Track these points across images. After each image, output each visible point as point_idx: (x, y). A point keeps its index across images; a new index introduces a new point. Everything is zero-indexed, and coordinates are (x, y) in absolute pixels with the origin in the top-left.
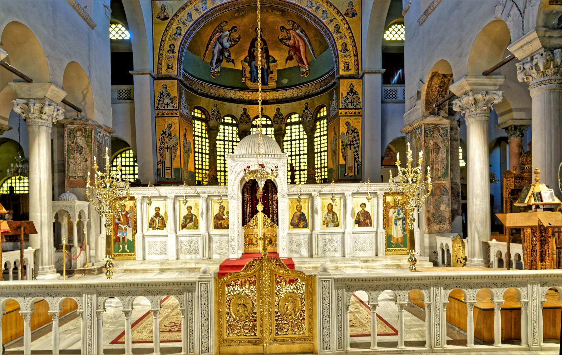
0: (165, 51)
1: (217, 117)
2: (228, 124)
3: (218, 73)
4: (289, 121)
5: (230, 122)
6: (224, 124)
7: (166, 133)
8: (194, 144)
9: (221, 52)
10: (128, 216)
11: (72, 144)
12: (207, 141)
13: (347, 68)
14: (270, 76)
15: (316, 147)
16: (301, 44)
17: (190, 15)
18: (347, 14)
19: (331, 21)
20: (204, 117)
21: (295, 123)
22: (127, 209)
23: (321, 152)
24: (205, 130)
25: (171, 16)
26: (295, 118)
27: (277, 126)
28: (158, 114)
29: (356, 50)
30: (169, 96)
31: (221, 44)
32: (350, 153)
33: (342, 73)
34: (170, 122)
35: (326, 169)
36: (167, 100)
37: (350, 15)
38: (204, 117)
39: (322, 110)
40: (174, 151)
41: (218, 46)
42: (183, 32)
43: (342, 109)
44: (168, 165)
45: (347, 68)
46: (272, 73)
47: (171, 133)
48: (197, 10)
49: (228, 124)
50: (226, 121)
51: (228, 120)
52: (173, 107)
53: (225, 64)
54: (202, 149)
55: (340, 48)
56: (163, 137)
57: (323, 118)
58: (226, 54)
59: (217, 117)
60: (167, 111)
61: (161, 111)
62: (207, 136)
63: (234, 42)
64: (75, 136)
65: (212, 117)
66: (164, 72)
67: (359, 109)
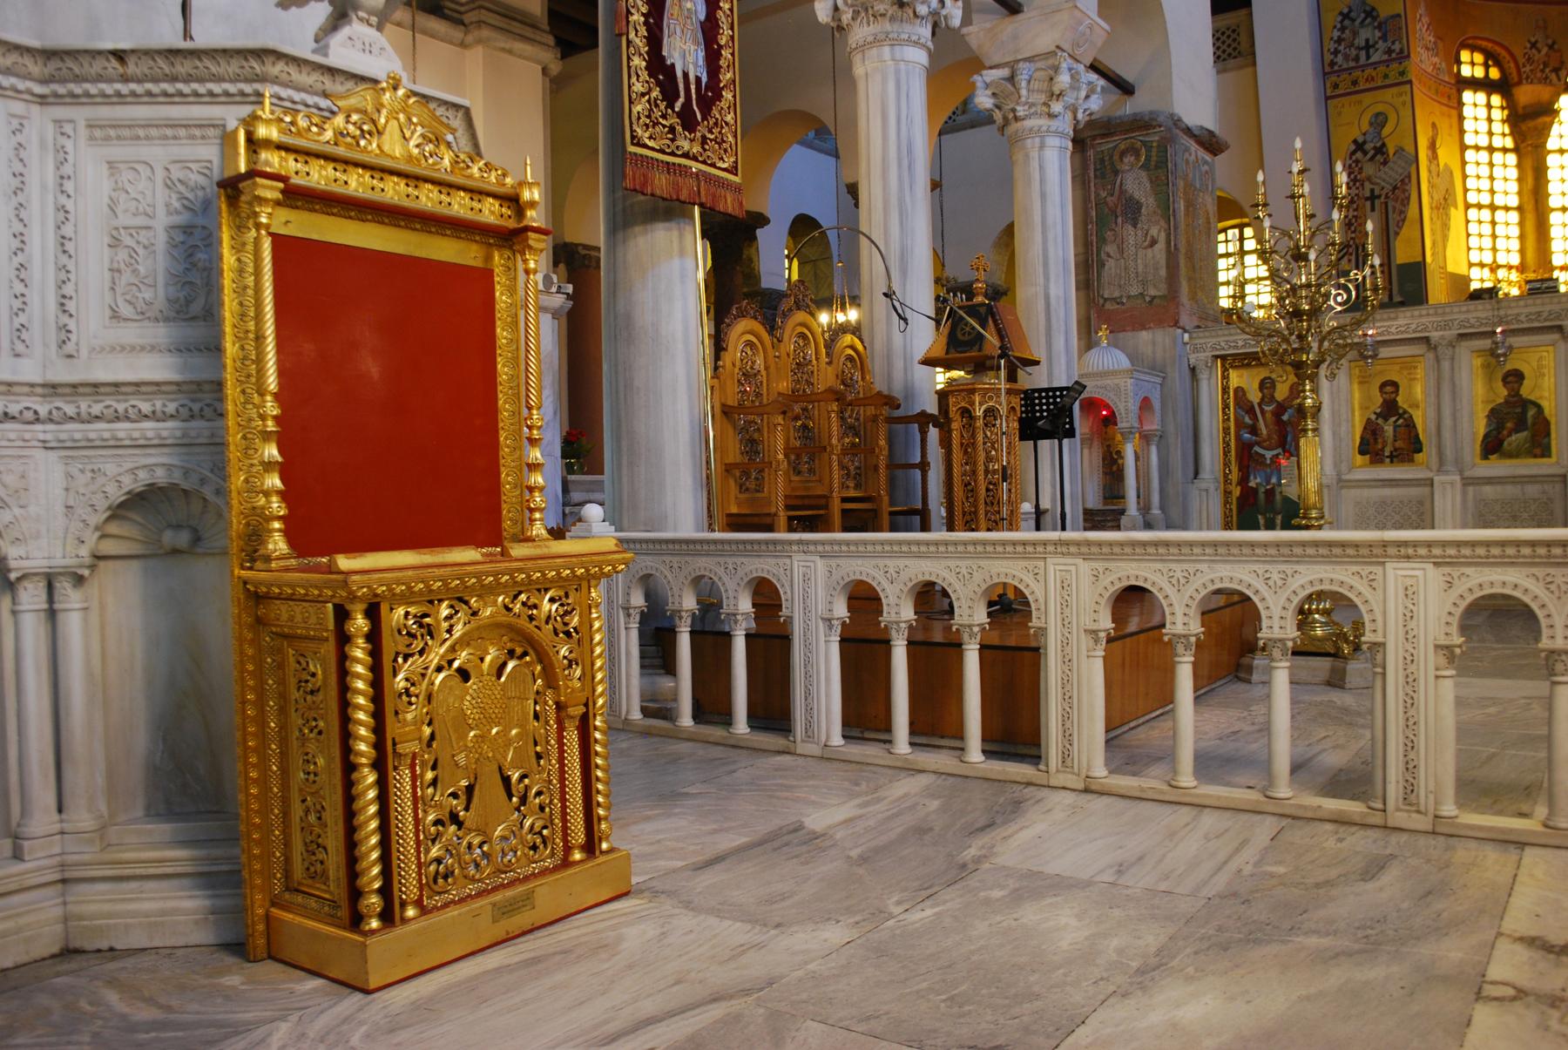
1: (1546, 65)
7: (1368, 146)
8: (1465, 177)
10: (1285, 417)
11: (1109, 199)
12: (1512, 159)
20: (1494, 73)
24: (1503, 121)
28: (1336, 86)
30: (1374, 18)
34: (1380, 108)
38: (1494, 73)
40: (1398, 206)
47: (1384, 145)
52: (1389, 51)
54: (1492, 192)
56: (1357, 162)
59: (1546, 65)
60: (1369, 71)
61: (1344, 75)
62: (1509, 143)
64: (1116, 172)
65: (1528, 68)
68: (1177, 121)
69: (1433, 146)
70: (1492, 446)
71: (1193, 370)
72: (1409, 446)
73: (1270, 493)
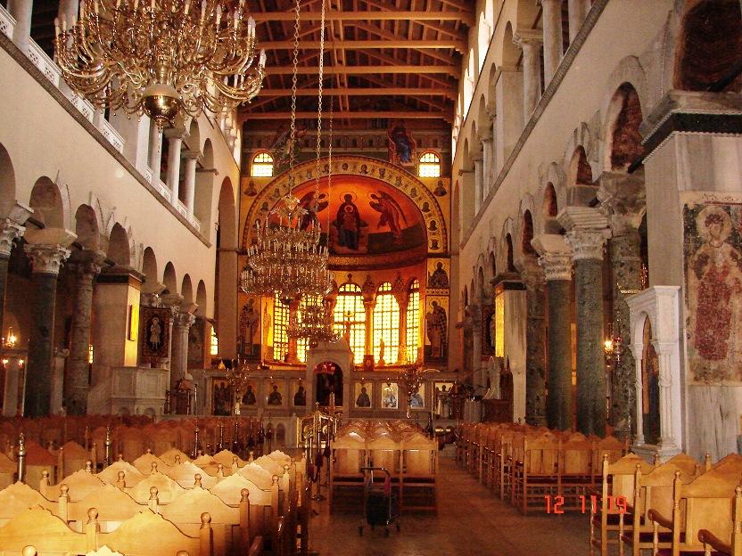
4: (381, 289)
14: (360, 241)
15: (408, 322)
17: (277, 191)
18: (435, 193)
19: (420, 199)
21: (387, 292)
26: (387, 287)
27: (367, 296)
29: (445, 229)
32: (436, 333)
33: (430, 251)
37: (439, 193)
39: (415, 282)
43: (428, 288)
44: (247, 341)
45: (435, 246)
46: (363, 236)
55: (428, 226)
57: (417, 290)
68: (206, 318)
69: (266, 310)
71: (206, 380)
72: (253, 401)
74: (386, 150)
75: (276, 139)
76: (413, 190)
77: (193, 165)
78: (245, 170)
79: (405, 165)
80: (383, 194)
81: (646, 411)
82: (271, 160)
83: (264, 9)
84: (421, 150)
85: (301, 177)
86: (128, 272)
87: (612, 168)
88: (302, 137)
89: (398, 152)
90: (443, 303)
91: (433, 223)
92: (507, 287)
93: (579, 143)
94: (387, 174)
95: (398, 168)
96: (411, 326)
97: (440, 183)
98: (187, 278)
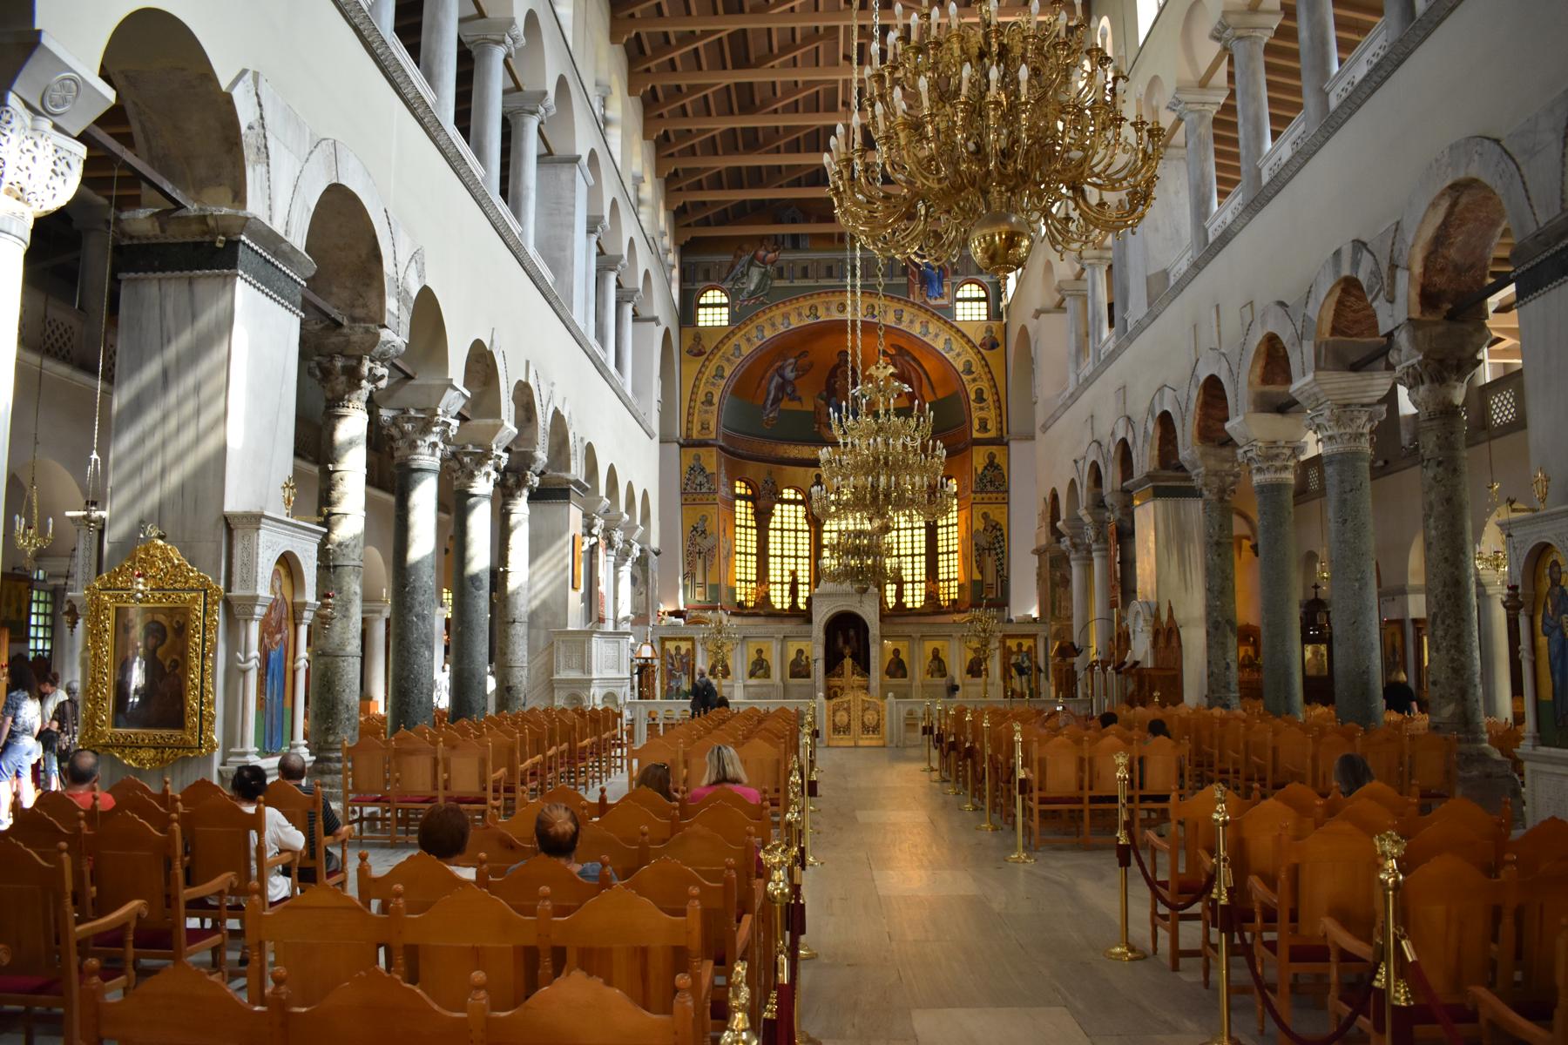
0: (698, 403)
2: (789, 502)
3: (774, 418)
5: (792, 497)
6: (783, 502)
9: (781, 388)
12: (755, 531)
13: (984, 427)
15: (940, 543)
16: (913, 375)
17: (738, 347)
19: (958, 355)
20: (749, 492)
22: (683, 652)
23: (948, 553)
25: (708, 351)
29: (999, 400)
31: (782, 377)
32: (990, 562)
33: (976, 435)
35: (956, 583)
36: (700, 479)
37: (988, 346)
41: (777, 380)
42: (727, 373)
43: (975, 492)
45: (984, 427)
48: (749, 340)
49: (789, 502)
50: (785, 496)
51: (788, 494)
53: (786, 405)
55: (973, 396)
58: (789, 390)
62: (754, 524)
63: (802, 371)
66: (695, 435)
67: (1003, 492)
70: (752, 674)
73: (678, 689)
74: (904, 280)
75: (733, 267)
76: (947, 341)
77: (628, 310)
78: (687, 310)
79: (933, 302)
80: (900, 349)
81: (1547, 694)
82: (725, 300)
83: (729, 64)
84: (959, 280)
85: (773, 325)
86: (569, 482)
87: (1422, 313)
88: (773, 263)
89: (922, 283)
90: (996, 513)
91: (980, 393)
92: (1159, 493)
93: (1346, 271)
94: (906, 317)
95: (922, 308)
96: (945, 549)
97: (989, 329)
98: (630, 485)
